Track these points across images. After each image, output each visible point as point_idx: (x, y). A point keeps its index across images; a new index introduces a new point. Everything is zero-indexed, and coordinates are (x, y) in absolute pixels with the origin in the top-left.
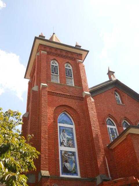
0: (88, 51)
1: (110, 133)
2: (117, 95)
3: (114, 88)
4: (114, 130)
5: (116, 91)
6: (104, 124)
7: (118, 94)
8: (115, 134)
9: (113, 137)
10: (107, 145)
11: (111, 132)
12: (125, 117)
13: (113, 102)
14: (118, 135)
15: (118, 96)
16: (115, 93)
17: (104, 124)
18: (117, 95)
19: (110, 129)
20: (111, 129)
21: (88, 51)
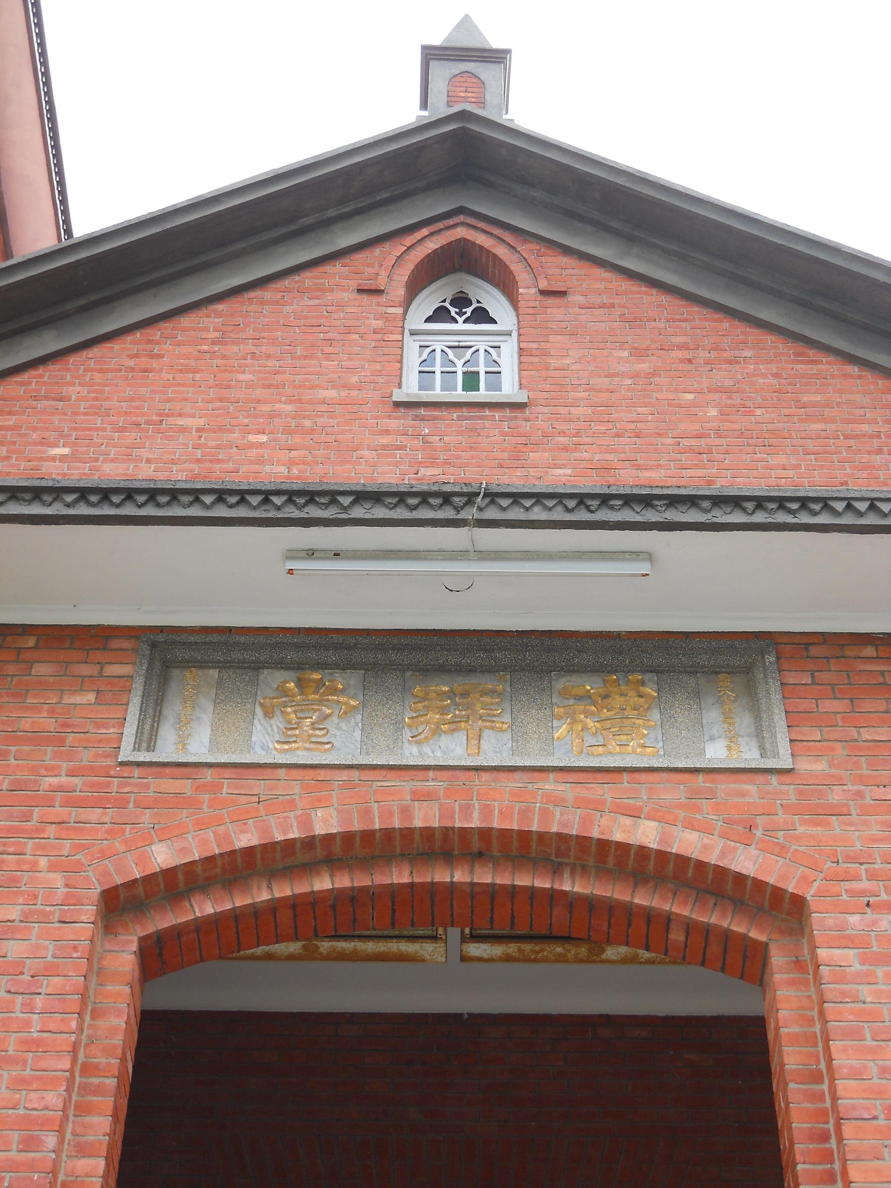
2: (482, 316)
3: (425, 232)
13: (331, 394)
16: (461, 301)
18: (482, 316)
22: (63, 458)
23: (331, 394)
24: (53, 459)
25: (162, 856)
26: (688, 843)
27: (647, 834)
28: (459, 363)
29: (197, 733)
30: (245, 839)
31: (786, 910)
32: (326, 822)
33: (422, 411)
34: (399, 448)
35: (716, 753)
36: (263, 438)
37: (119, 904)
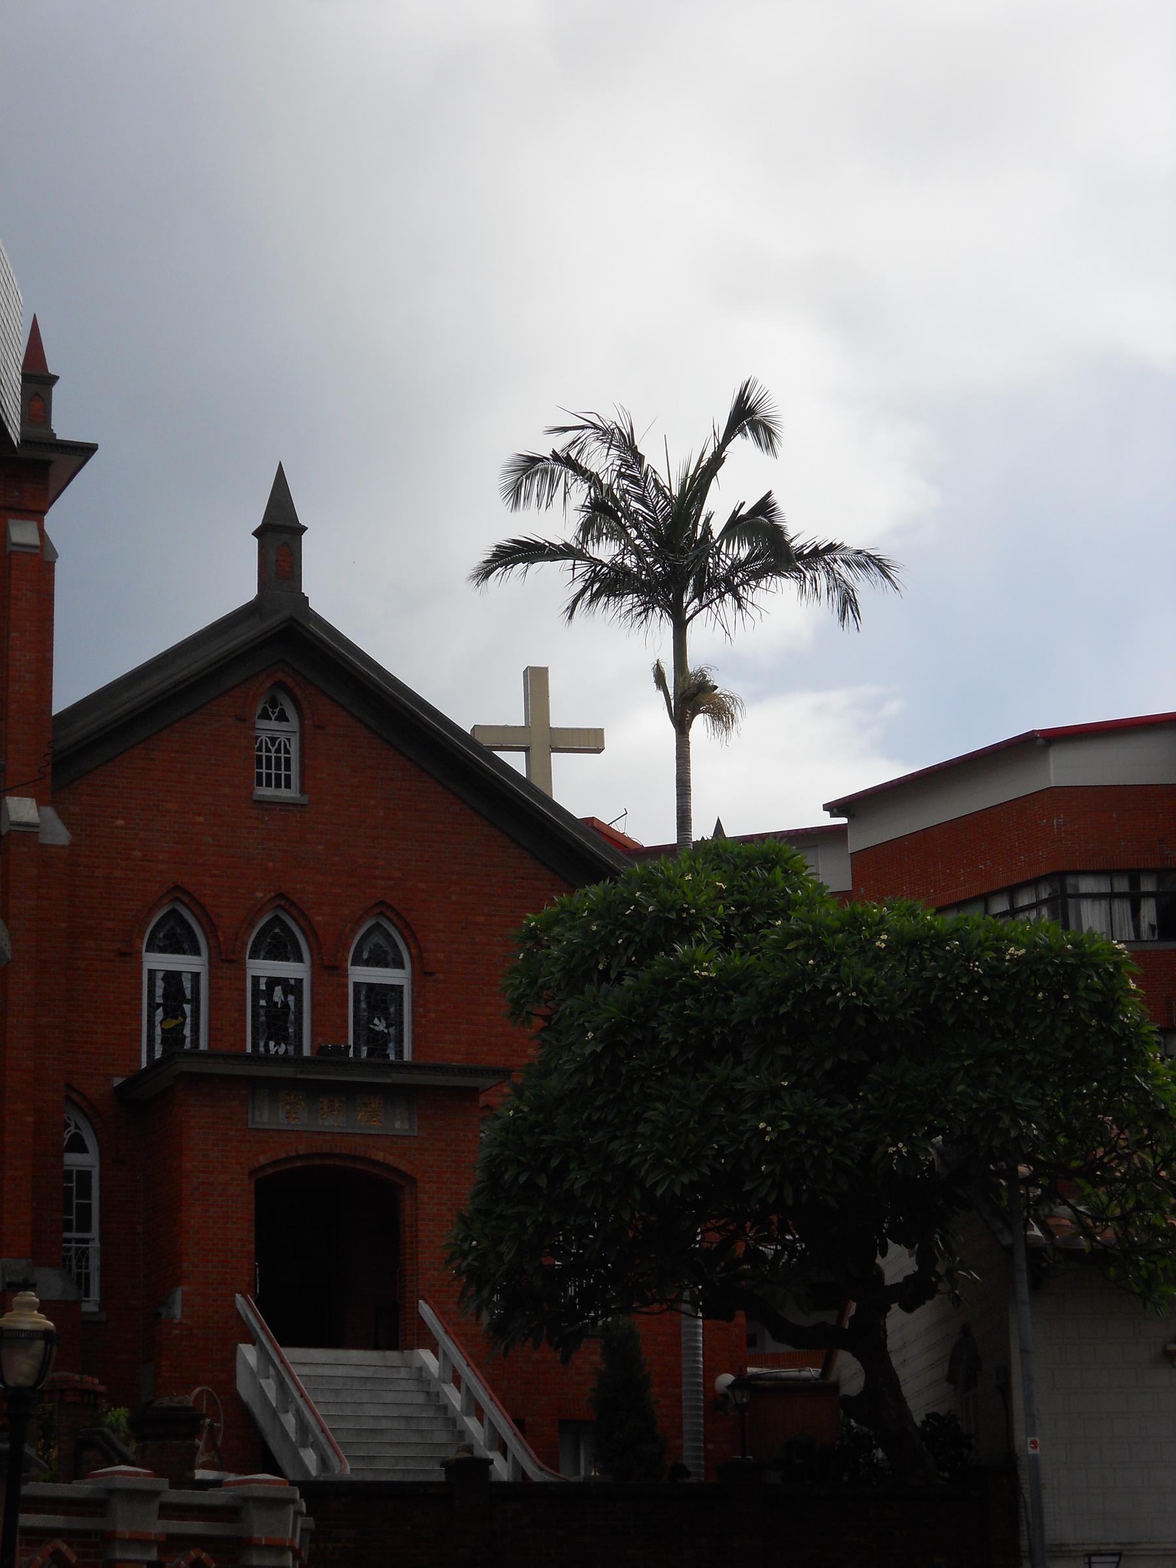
0: (88, 450)
1: (159, 1005)
4: (187, 985)
5: (280, 685)
6: (125, 954)
7: (291, 712)
8: (187, 1008)
9: (171, 1024)
10: (117, 1081)
11: (164, 996)
12: (281, 895)
13: (227, 790)
14: (158, 1055)
15: (293, 724)
16: (274, 703)
17: (125, 954)
18: (282, 717)
19: (160, 975)
20: (172, 978)
21: (88, 450)
22: (122, 827)
23: (227, 790)
24: (117, 827)
25: (262, 1160)
26: (391, 1160)
27: (379, 1156)
28: (273, 750)
29: (267, 1116)
30: (283, 1156)
31: (412, 1180)
32: (302, 1150)
33: (265, 806)
34: (256, 828)
35: (400, 1125)
36: (201, 819)
37: (252, 1173)
